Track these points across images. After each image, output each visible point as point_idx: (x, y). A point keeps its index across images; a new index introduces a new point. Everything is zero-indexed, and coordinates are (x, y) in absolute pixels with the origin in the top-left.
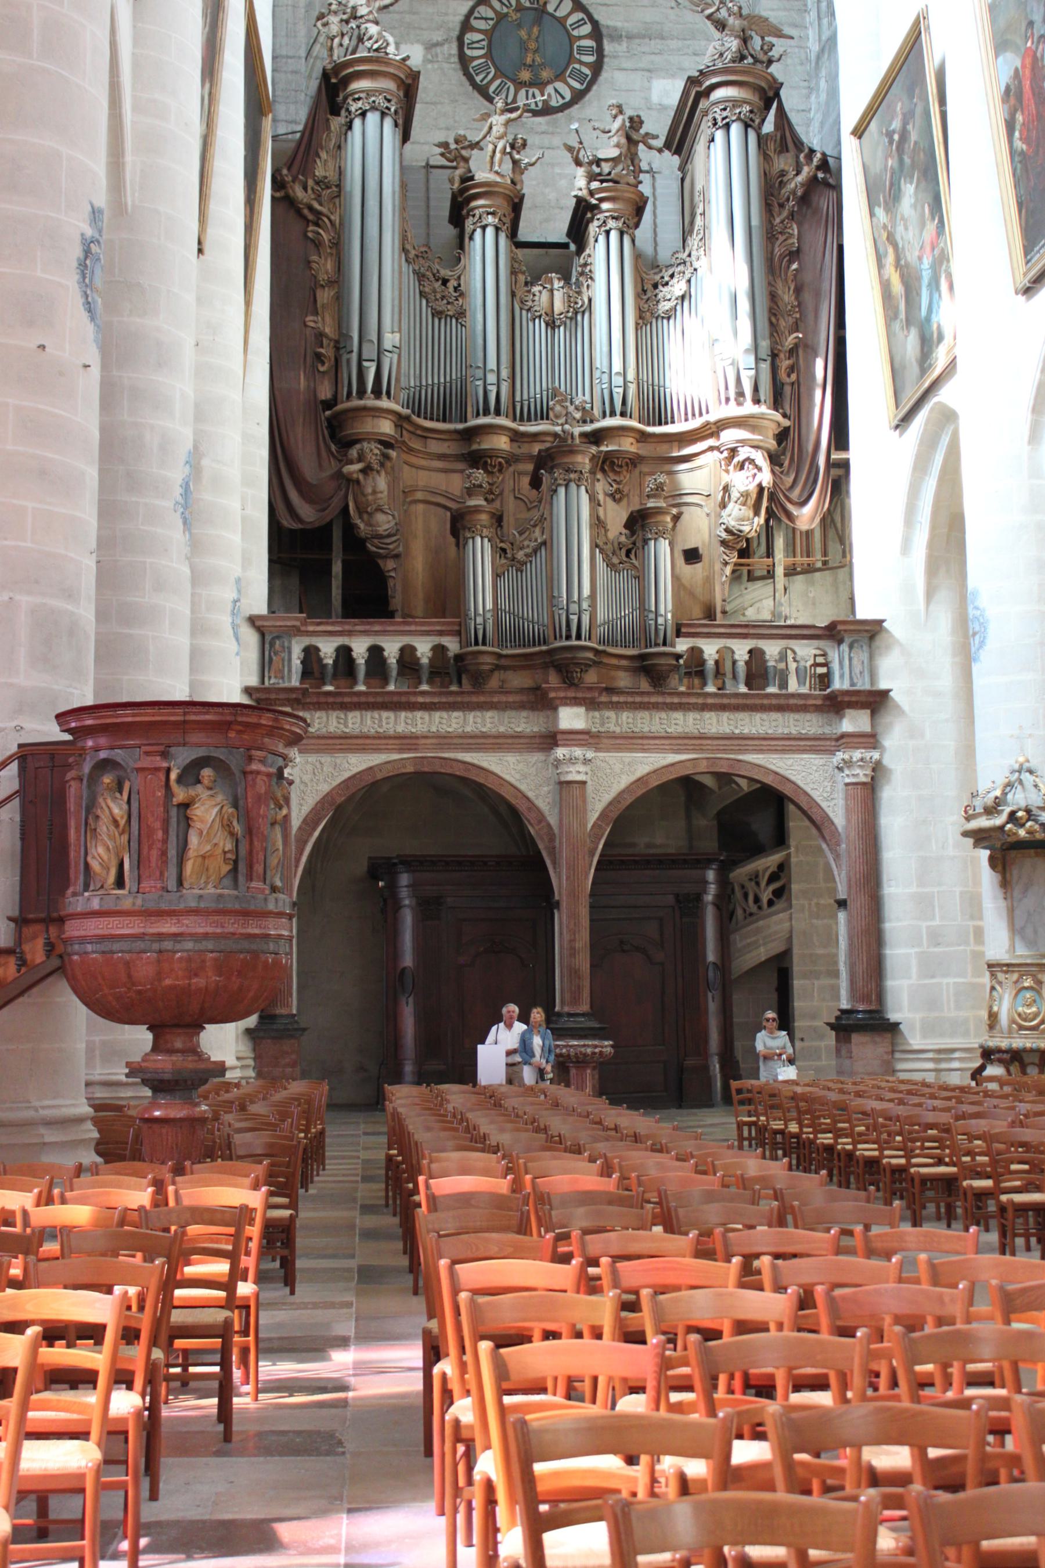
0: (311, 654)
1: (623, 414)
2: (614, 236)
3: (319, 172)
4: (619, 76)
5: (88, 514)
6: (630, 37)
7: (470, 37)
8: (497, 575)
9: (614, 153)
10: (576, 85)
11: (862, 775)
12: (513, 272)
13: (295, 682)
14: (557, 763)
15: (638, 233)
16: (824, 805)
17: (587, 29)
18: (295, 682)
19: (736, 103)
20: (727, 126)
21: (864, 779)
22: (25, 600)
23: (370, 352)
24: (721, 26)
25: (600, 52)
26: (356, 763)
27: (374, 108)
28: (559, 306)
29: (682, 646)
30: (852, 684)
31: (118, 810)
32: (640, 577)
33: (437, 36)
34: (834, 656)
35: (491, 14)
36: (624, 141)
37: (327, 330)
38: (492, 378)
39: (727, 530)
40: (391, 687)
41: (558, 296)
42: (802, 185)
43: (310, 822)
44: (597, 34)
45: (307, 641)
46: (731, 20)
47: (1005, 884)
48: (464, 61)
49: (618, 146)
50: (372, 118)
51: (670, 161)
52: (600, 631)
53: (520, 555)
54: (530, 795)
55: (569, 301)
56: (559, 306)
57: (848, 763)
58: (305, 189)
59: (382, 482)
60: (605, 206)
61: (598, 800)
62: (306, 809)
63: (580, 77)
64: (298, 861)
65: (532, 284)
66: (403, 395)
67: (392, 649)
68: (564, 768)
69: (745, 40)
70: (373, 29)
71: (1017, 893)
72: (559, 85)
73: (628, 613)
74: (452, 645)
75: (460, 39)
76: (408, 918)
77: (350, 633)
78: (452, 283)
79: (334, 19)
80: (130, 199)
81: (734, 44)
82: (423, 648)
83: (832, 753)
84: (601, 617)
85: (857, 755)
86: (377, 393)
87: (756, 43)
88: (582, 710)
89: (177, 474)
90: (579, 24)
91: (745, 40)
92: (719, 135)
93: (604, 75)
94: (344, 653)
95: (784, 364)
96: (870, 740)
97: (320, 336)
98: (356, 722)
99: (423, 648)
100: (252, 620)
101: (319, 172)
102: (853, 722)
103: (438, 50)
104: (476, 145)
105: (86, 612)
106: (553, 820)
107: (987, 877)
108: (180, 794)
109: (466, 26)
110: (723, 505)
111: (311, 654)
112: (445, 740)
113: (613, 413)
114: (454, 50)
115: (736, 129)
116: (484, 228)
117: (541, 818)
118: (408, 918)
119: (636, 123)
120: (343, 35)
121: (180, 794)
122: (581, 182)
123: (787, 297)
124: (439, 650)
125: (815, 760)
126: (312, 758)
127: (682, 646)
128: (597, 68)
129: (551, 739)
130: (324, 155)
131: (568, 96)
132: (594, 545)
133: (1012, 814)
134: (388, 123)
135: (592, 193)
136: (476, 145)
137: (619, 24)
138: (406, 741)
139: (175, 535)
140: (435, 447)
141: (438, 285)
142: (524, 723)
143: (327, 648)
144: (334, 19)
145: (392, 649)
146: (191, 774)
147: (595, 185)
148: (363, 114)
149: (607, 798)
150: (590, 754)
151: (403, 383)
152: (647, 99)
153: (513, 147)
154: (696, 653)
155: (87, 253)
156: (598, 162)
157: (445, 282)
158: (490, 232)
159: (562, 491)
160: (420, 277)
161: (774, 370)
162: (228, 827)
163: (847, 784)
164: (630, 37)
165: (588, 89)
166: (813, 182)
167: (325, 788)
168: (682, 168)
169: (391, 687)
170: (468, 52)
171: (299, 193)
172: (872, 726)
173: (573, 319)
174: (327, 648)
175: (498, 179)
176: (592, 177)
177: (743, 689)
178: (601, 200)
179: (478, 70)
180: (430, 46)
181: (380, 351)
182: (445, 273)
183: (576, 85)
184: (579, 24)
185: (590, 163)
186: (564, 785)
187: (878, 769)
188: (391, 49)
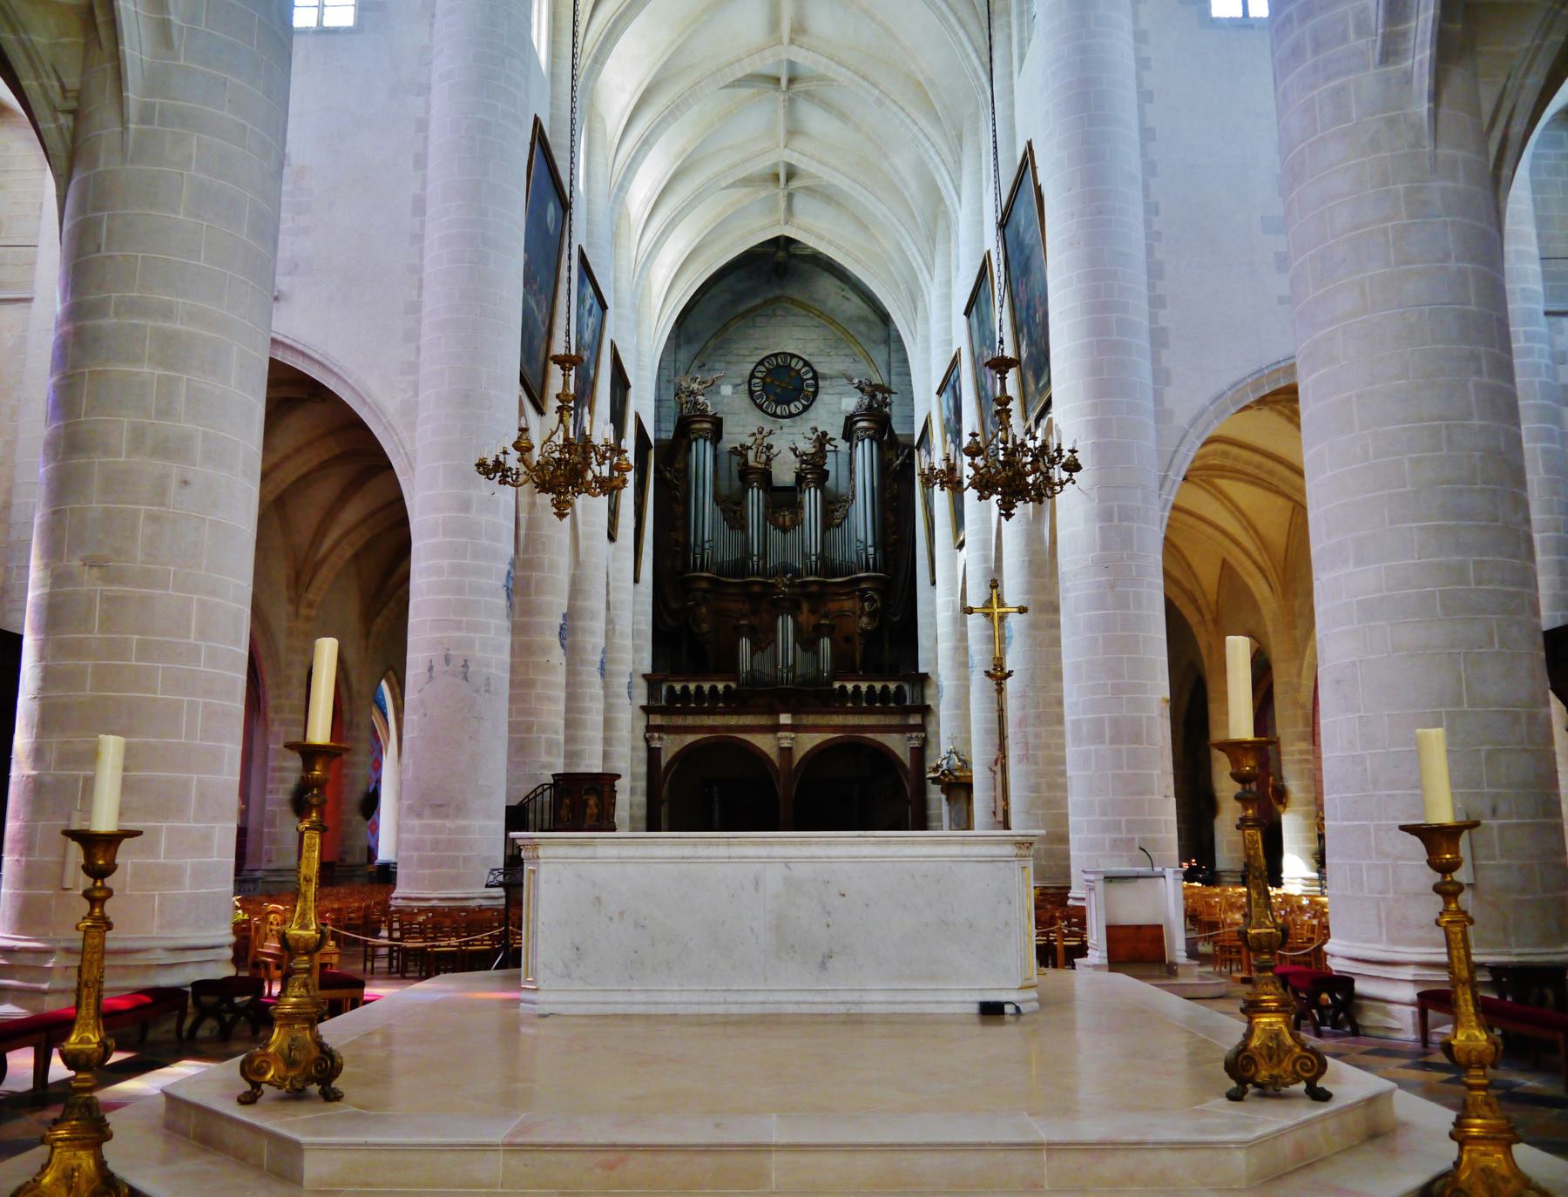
0: (671, 689)
1: (816, 574)
2: (813, 489)
3: (677, 466)
4: (826, 397)
5: (561, 707)
6: (831, 378)
7: (755, 381)
8: (753, 654)
9: (813, 450)
10: (805, 403)
11: (916, 743)
12: (766, 507)
13: (663, 703)
14: (779, 739)
15: (830, 483)
16: (901, 756)
17: (810, 375)
18: (663, 703)
19: (866, 429)
20: (863, 440)
21: (917, 745)
22: (544, 736)
23: (698, 550)
24: (862, 390)
25: (817, 386)
26: (690, 739)
27: (701, 437)
28: (788, 522)
29: (837, 685)
30: (913, 702)
31: (567, 801)
32: (816, 653)
33: (739, 381)
34: (907, 688)
35: (764, 370)
36: (817, 444)
37: (680, 539)
38: (755, 558)
39: (861, 629)
40: (706, 705)
41: (787, 518)
42: (900, 465)
43: (670, 764)
44: (816, 376)
45: (669, 684)
46: (867, 388)
47: (948, 799)
48: (751, 393)
49: (814, 447)
50: (701, 441)
51: (843, 446)
52: (799, 680)
53: (763, 645)
54: (768, 752)
55: (791, 518)
56: (788, 522)
57: (910, 738)
58: (670, 472)
59: (704, 610)
60: (809, 476)
61: (798, 755)
62: (668, 759)
63: (806, 398)
64: (665, 781)
65: (776, 513)
66: (715, 568)
67: (706, 687)
68: (782, 741)
69: (873, 397)
70: (701, 399)
71: (952, 803)
72: (797, 403)
73: (811, 671)
74: (733, 685)
75: (750, 382)
76: (717, 807)
77: (688, 681)
78: (738, 513)
79: (683, 396)
80: (582, 557)
81: (866, 401)
82: (720, 686)
83: (905, 733)
84: (798, 671)
85: (914, 735)
86: (702, 570)
87: (880, 396)
88: (790, 715)
89: (598, 658)
90: (806, 373)
91: (873, 397)
92: (860, 444)
93: (819, 397)
94: (685, 689)
95: (890, 549)
96: (922, 728)
97: (677, 542)
98: (690, 721)
99: (720, 686)
100: (644, 676)
101: (677, 466)
102: (915, 720)
103: (739, 388)
104: (750, 448)
105: (561, 737)
106: (777, 764)
107: (943, 797)
108: (585, 797)
109: (752, 376)
110: (860, 617)
111: (671, 689)
112: (730, 728)
113: (811, 574)
114: (747, 388)
115: (866, 441)
116: (753, 488)
117: (772, 763)
118: (717, 807)
119: (824, 434)
120: (687, 402)
121: (585, 797)
122: (798, 466)
123: (892, 518)
124: (727, 688)
125: (896, 736)
126: (672, 737)
127: (837, 685)
128: (815, 394)
129: (776, 728)
130: (679, 457)
131: (801, 408)
132: (795, 642)
133: (943, 772)
134: (708, 443)
135: (802, 470)
136: (750, 448)
137: (826, 372)
138: (712, 729)
139: (598, 679)
140: (731, 590)
141: (732, 514)
142: (763, 720)
143: (678, 687)
144: (683, 396)
145: (706, 687)
146: (587, 793)
147: (804, 466)
148: (696, 440)
149: (802, 753)
150: (793, 735)
151: (714, 561)
152: (840, 408)
153: (767, 447)
154: (843, 688)
155: (561, 628)
156: (806, 455)
157: (735, 512)
158: (755, 490)
159: (781, 618)
160: (723, 511)
161: (885, 553)
162: (597, 806)
163: (912, 748)
164: (831, 378)
165: (811, 405)
166: (903, 463)
167: (676, 749)
168: (851, 448)
169: (706, 705)
170: (754, 389)
171: (668, 475)
172: (923, 721)
173: (794, 529)
174: (678, 687)
175: (759, 466)
176: (803, 462)
177: (864, 705)
178: (806, 474)
179: (758, 398)
180: (735, 386)
181: (703, 549)
182: (735, 508)
183: (805, 403)
184: (806, 373)
185: (802, 456)
186: (782, 749)
187: (925, 741)
188: (709, 409)
